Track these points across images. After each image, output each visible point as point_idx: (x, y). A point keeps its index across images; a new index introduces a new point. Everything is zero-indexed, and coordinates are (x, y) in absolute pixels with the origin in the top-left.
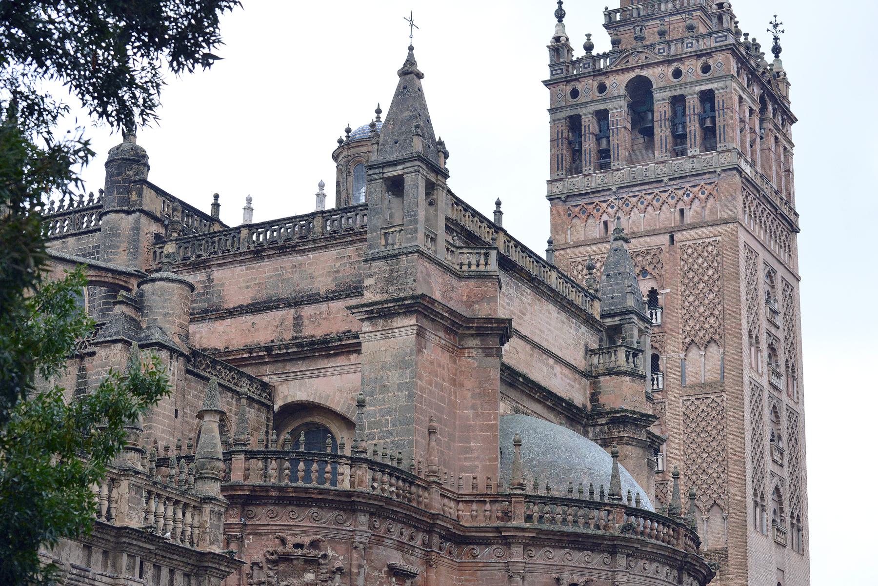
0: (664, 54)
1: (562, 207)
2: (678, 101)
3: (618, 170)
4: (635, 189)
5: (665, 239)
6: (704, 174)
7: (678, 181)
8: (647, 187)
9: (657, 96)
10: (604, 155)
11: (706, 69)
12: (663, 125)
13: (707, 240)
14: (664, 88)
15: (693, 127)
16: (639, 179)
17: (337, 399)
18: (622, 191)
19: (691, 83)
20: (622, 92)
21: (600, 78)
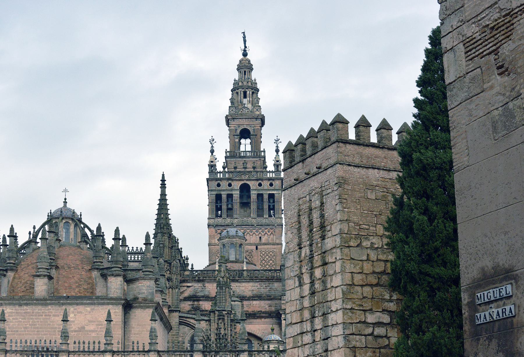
0: (255, 176)
1: (213, 230)
2: (260, 196)
3: (236, 218)
4: (243, 227)
5: (255, 247)
6: (270, 225)
7: (260, 226)
8: (248, 227)
9: (252, 192)
10: (229, 210)
11: (271, 185)
12: (255, 204)
13: (270, 250)
14: (255, 190)
15: (266, 206)
16: (245, 223)
17: (258, 332)
18: (238, 226)
19: (266, 190)
20: (239, 189)
21: (230, 181)
